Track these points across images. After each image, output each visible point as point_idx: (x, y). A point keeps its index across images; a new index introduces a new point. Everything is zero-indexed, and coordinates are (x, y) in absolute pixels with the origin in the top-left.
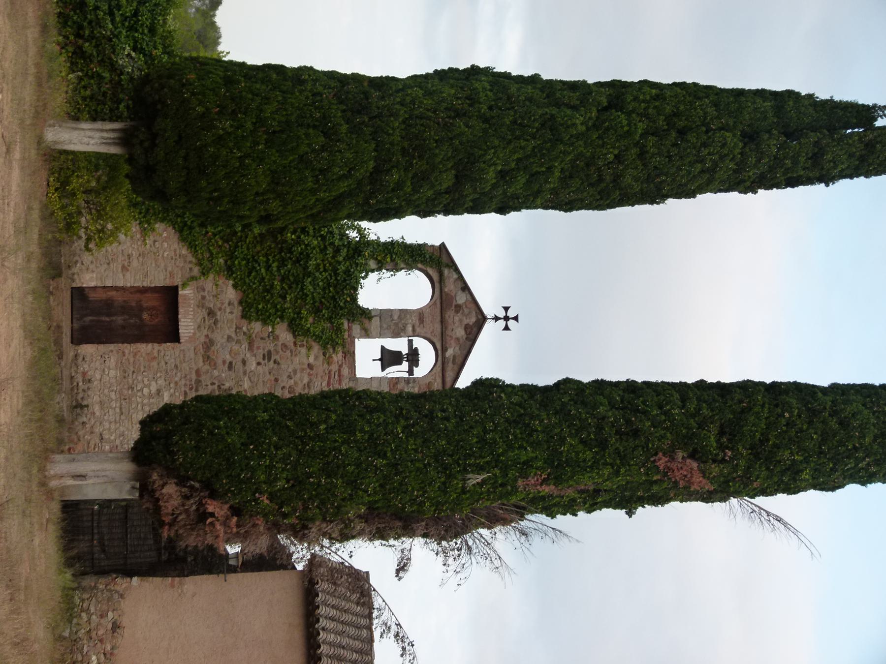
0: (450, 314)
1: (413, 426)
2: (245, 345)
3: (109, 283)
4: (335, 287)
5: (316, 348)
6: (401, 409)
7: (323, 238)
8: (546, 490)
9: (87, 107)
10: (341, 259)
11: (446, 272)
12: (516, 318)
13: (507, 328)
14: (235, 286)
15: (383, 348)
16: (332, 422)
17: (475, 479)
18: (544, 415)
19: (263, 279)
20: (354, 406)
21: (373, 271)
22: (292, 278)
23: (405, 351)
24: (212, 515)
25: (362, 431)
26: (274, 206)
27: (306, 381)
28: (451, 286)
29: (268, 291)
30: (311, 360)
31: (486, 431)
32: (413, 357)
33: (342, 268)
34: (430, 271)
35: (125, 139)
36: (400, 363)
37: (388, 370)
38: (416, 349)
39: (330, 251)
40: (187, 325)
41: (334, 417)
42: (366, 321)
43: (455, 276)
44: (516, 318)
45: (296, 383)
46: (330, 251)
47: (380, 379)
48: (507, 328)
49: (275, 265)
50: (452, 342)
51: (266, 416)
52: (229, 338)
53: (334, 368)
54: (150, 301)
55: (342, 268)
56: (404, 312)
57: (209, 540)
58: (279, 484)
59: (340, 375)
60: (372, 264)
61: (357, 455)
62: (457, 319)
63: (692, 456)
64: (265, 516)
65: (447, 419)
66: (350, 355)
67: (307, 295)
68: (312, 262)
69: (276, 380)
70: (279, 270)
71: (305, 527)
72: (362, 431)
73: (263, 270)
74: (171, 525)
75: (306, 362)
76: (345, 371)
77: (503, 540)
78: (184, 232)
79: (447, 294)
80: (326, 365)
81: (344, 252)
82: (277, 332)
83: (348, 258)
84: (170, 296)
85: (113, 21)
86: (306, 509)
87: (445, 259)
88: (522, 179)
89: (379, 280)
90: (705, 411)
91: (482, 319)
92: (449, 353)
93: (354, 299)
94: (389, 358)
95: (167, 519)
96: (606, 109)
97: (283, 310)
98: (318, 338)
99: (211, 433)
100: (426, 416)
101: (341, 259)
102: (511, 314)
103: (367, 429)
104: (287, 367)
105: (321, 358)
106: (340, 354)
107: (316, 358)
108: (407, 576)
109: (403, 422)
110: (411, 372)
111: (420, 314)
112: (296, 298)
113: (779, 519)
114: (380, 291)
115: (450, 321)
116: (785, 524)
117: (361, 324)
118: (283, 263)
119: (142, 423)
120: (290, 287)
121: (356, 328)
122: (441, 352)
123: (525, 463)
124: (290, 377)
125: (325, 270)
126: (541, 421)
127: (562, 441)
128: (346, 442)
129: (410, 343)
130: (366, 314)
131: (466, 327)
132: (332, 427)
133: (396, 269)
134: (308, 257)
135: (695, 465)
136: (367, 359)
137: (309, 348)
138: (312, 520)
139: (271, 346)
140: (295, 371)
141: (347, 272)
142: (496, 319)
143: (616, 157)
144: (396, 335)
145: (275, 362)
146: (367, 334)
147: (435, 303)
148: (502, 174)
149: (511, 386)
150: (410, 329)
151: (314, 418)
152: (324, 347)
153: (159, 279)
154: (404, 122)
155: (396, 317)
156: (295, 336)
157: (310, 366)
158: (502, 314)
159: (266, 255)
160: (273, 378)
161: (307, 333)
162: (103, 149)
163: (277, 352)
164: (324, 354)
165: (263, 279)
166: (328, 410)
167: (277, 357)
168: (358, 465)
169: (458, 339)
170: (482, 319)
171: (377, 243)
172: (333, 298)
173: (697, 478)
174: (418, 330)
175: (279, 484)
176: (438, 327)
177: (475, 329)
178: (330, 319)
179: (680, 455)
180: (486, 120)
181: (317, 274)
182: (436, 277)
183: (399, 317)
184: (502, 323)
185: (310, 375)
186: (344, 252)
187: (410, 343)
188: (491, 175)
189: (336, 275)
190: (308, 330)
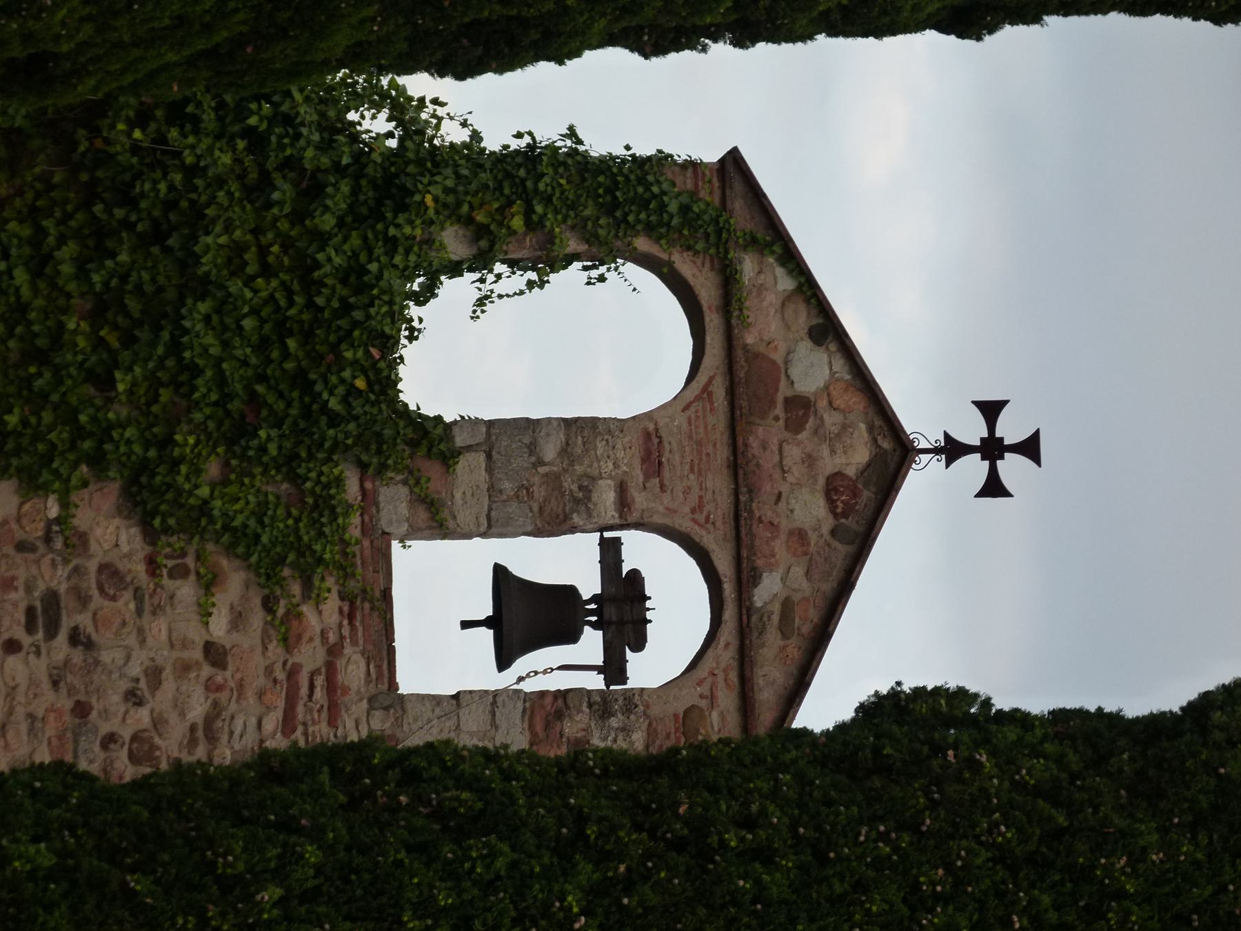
0: (767, 433)
1: (628, 885)
4: (307, 336)
5: (235, 582)
6: (581, 820)
7: (257, 141)
10: (327, 222)
11: (748, 266)
12: (1030, 448)
13: (993, 488)
15: (500, 573)
19: (22, 308)
20: (394, 808)
21: (455, 270)
22: (133, 304)
23: (589, 585)
27: (198, 710)
28: (769, 322)
29: (41, 357)
30: (219, 627)
32: (623, 608)
33: (333, 259)
34: (685, 265)
36: (571, 637)
37: (523, 664)
38: (635, 575)
39: (283, 191)
41: (312, 854)
42: (432, 469)
43: (786, 283)
44: (1030, 448)
45: (158, 722)
46: (283, 191)
47: (493, 698)
48: (993, 488)
49: (69, 250)
50: (779, 546)
51: (44, 855)
53: (310, 656)
55: (333, 259)
56: (583, 431)
59: (332, 687)
60: (454, 242)
62: (793, 453)
65: (764, 855)
66: (373, 607)
67: (196, 371)
68: (213, 241)
69: (82, 710)
70: (82, 273)
73: (21, 276)
75: (197, 636)
76: (354, 671)
79: (754, 357)
80: (275, 650)
81: (339, 195)
82: (82, 518)
83: (352, 220)
87: (741, 218)
89: (481, 302)
91: (895, 454)
92: (768, 590)
93: (386, 383)
94: (526, 614)
97: (105, 432)
98: (240, 541)
100: (679, 845)
101: (327, 222)
103: (444, 900)
104: (124, 658)
105: (257, 618)
106: (332, 604)
107: (238, 620)
109: (586, 871)
110: (614, 668)
111: (647, 433)
112: (155, 384)
114: (491, 349)
115: (769, 461)
117: (414, 480)
118: (98, 242)
120: (129, 340)
121: (394, 500)
122: (730, 590)
124: (134, 698)
125: (267, 271)
126: (1138, 857)
129: (610, 552)
130: (432, 438)
131: (834, 486)
132: (308, 897)
133: (545, 261)
134: (197, 221)
136: (438, 617)
137: (210, 583)
139: (56, 578)
140: (154, 675)
141: (354, 275)
142: (952, 450)
144: (552, 524)
145: (75, 638)
146: (438, 523)
147: (706, 391)
149: (1017, 718)
150: (606, 497)
152: (267, 576)
155: (550, 451)
156: (150, 535)
157: (215, 654)
159: (33, 215)
160: (67, 704)
161: (197, 519)
163: (83, 600)
164: (268, 605)
165: (22, 308)
166: (287, 825)
167: (84, 620)
169: (800, 535)
170: (895, 454)
171: (472, 153)
172: (301, 380)
174: (640, 500)
176: (719, 485)
177: (867, 495)
178: (288, 464)
181: (235, 286)
182: (707, 288)
183: (565, 451)
185: (211, 687)
186: (339, 195)
187: (610, 552)
189: (311, 287)
190: (204, 508)
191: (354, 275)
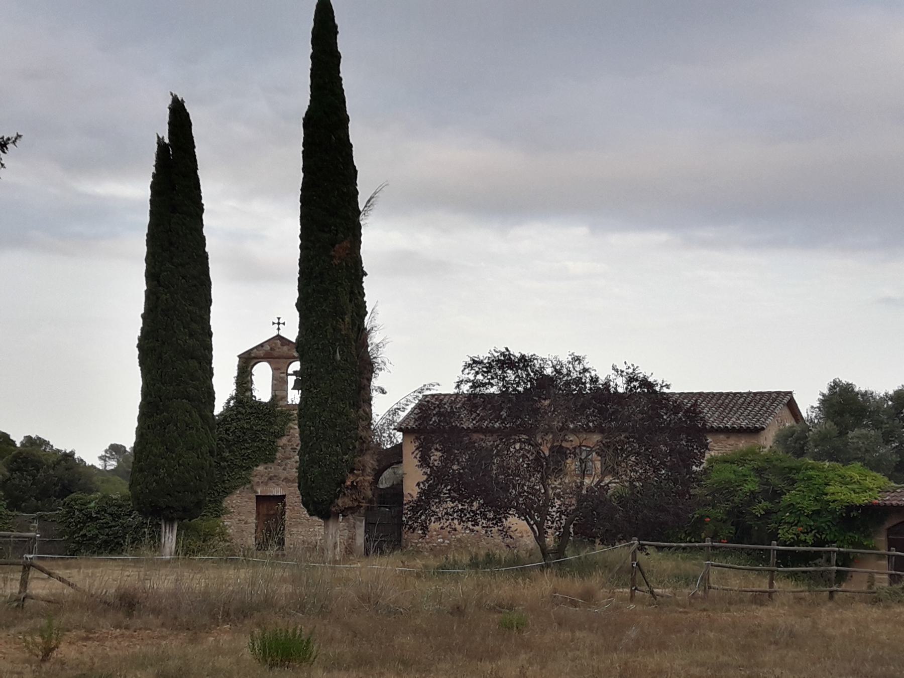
0: (275, 354)
2: (288, 461)
3: (253, 531)
5: (291, 424)
7: (232, 420)
8: (347, 319)
9: (156, 543)
12: (279, 319)
14: (257, 466)
16: (311, 424)
17: (338, 357)
18: (312, 319)
24: (352, 482)
25: (315, 409)
26: (205, 449)
28: (261, 353)
29: (260, 449)
31: (318, 349)
35: (170, 521)
39: (239, 416)
40: (277, 491)
46: (239, 416)
52: (284, 469)
54: (264, 510)
55: (249, 410)
57: (367, 484)
58: (338, 449)
60: (248, 394)
61: (326, 413)
63: (333, 246)
64: (355, 457)
71: (361, 438)
72: (315, 409)
74: (359, 502)
77: (374, 339)
78: (227, 492)
81: (240, 409)
84: (261, 499)
85: (115, 526)
86: (351, 437)
87: (245, 356)
88: (194, 326)
90: (312, 238)
91: (279, 337)
95: (356, 504)
96: (158, 281)
98: (286, 423)
99: (313, 482)
102: (276, 321)
108: (386, 390)
111: (274, 369)
113: (369, 201)
114: (262, 390)
116: (371, 198)
118: (245, 441)
119: (311, 515)
121: (281, 403)
123: (334, 330)
127: (324, 310)
128: (320, 417)
130: (274, 397)
135: (337, 246)
138: (357, 434)
141: (251, 407)
142: (279, 329)
143: (183, 278)
146: (285, 397)
148: (191, 335)
151: (308, 432)
153: (252, 505)
154: (163, 384)
158: (276, 326)
162: (175, 532)
168: (331, 412)
170: (279, 337)
171: (237, 390)
173: (346, 244)
175: (338, 449)
179: (333, 253)
180: (164, 343)
184: (281, 326)
186: (240, 409)
188: (190, 342)
191: (251, 407)
